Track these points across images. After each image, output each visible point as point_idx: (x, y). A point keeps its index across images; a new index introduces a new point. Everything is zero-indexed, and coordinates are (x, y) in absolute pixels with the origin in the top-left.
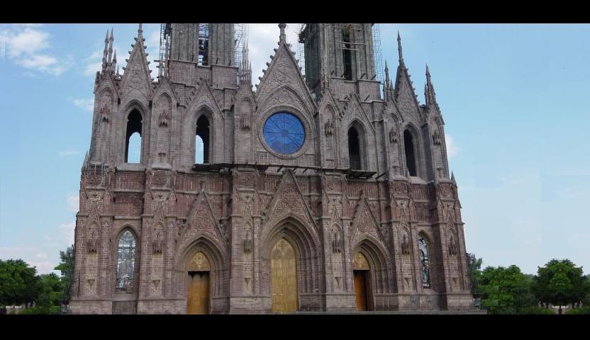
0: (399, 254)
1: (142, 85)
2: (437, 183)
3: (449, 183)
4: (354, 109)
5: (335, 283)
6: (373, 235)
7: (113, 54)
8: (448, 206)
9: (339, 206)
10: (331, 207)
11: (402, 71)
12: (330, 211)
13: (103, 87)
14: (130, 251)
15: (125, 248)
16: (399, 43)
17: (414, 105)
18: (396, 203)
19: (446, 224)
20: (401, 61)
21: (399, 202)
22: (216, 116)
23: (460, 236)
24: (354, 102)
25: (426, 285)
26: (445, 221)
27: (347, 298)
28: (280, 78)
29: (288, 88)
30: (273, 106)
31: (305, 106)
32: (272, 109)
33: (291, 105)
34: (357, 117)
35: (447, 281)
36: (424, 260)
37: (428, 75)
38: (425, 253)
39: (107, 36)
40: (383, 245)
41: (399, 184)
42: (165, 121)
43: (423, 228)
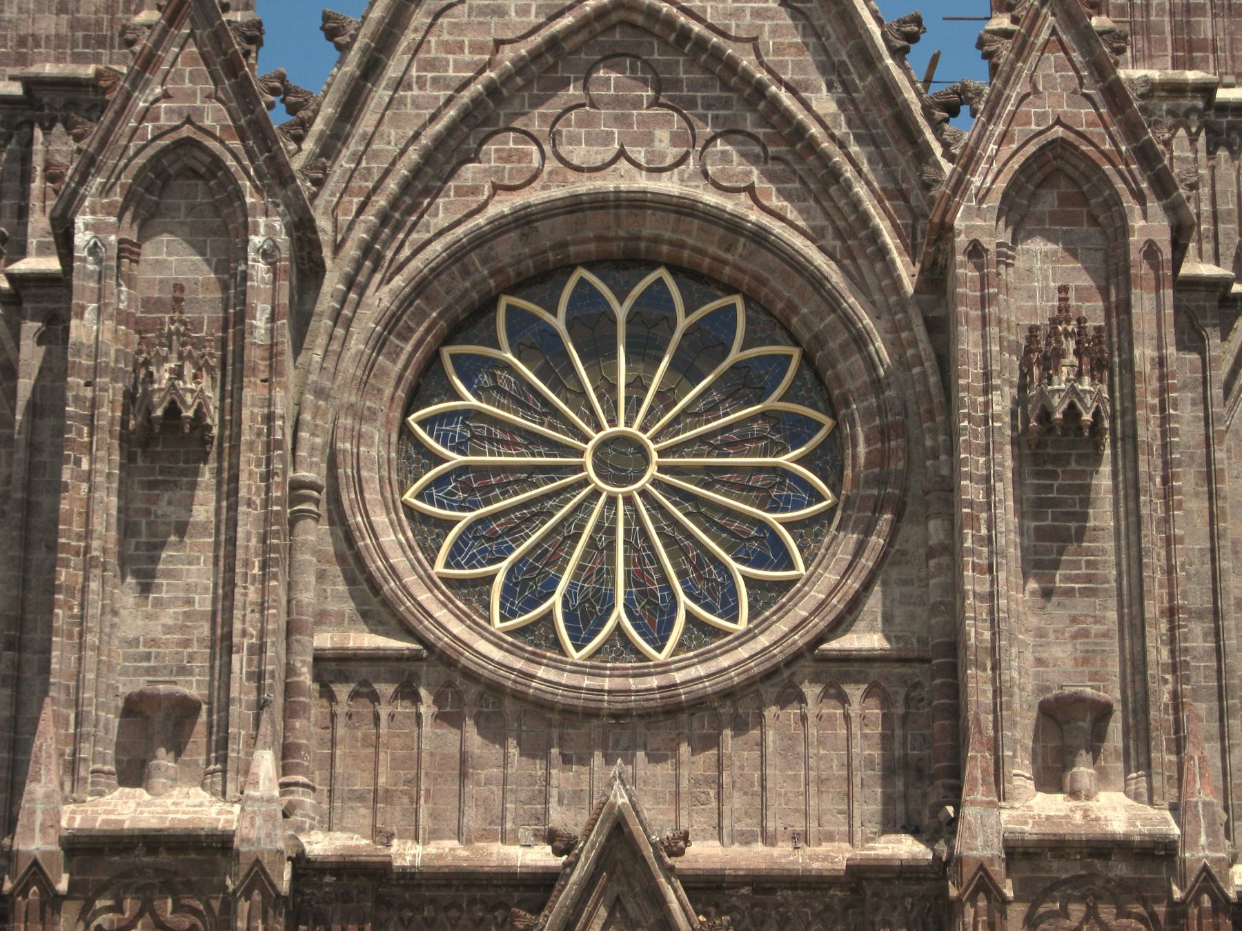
30: (503, 206)
32: (479, 240)
33: (668, 185)
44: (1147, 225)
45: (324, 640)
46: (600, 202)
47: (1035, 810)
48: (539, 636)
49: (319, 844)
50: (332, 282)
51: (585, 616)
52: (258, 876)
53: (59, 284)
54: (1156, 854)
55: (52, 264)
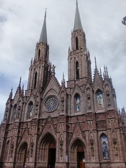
0: (88, 144)
5: (60, 158)
6: (81, 137)
8: (112, 121)
9: (63, 127)
10: (60, 127)
12: (60, 129)
18: (87, 122)
19: (110, 129)
21: (89, 122)
25: (107, 158)
26: (110, 128)
27: (63, 164)
28: (50, 87)
29: (51, 89)
33: (53, 94)
34: (77, 92)
36: (106, 146)
38: (107, 143)
41: (90, 115)
43: (103, 132)
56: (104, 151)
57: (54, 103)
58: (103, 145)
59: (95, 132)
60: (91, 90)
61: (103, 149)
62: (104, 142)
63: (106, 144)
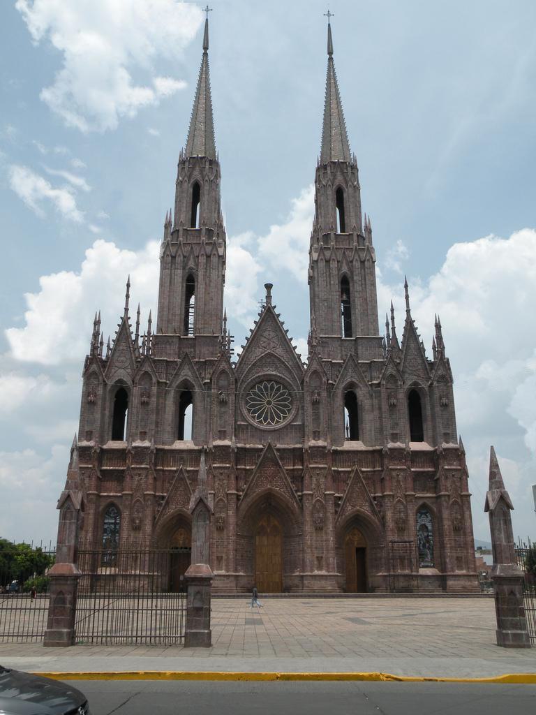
0: (392, 530)
1: (127, 364)
2: (441, 449)
3: (456, 450)
4: (350, 370)
6: (366, 509)
7: (100, 336)
11: (410, 324)
13: (91, 371)
14: (115, 526)
15: (110, 524)
16: (407, 291)
17: (420, 362)
20: (408, 311)
22: (197, 390)
23: (465, 509)
24: (351, 362)
29: (270, 355)
31: (291, 372)
33: (274, 373)
34: (353, 380)
35: (448, 560)
37: (438, 327)
38: (430, 528)
39: (96, 318)
40: (376, 520)
42: (145, 399)
43: (425, 501)
44: (324, 379)
45: (238, 423)
46: (267, 375)
47: (312, 443)
48: (261, 422)
49: (239, 445)
50: (239, 384)
51: (266, 420)
52: (233, 450)
53: (211, 383)
54: (324, 447)
55: (209, 381)
56: (421, 548)
57: (279, 401)
58: (421, 533)
59: (409, 502)
60: (399, 383)
61: (420, 543)
62: (424, 525)
63: (428, 531)
